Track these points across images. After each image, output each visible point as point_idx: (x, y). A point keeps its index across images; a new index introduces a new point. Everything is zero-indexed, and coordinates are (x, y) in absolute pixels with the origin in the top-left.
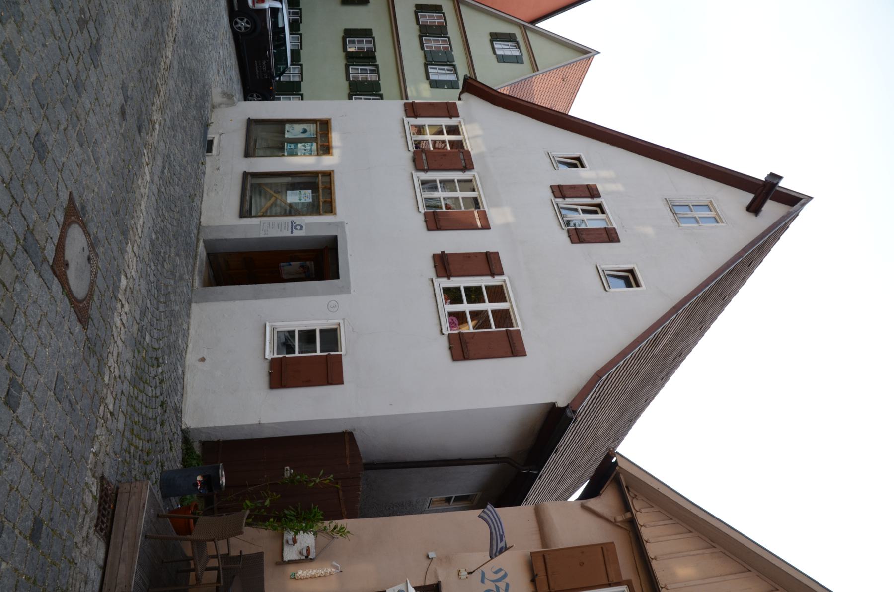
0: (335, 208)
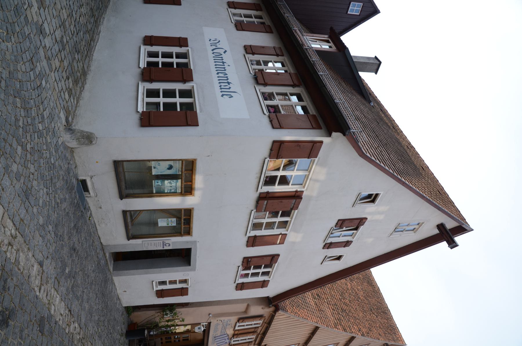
0: (192, 232)
